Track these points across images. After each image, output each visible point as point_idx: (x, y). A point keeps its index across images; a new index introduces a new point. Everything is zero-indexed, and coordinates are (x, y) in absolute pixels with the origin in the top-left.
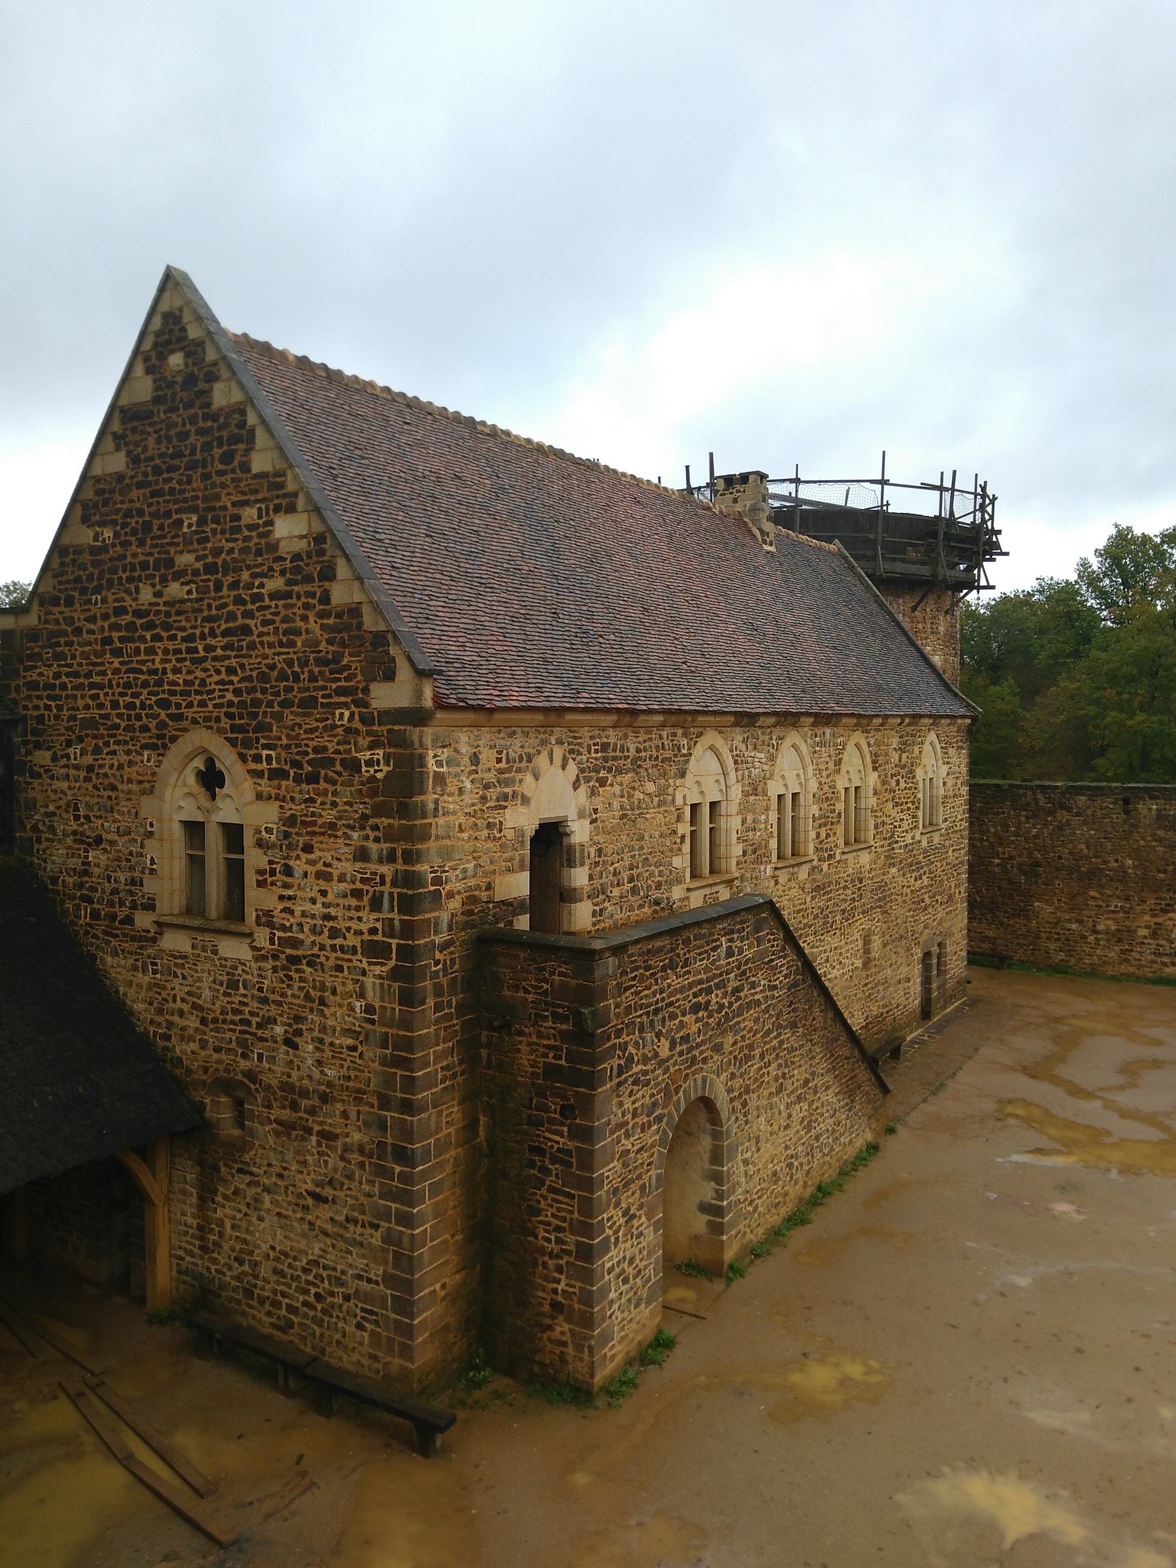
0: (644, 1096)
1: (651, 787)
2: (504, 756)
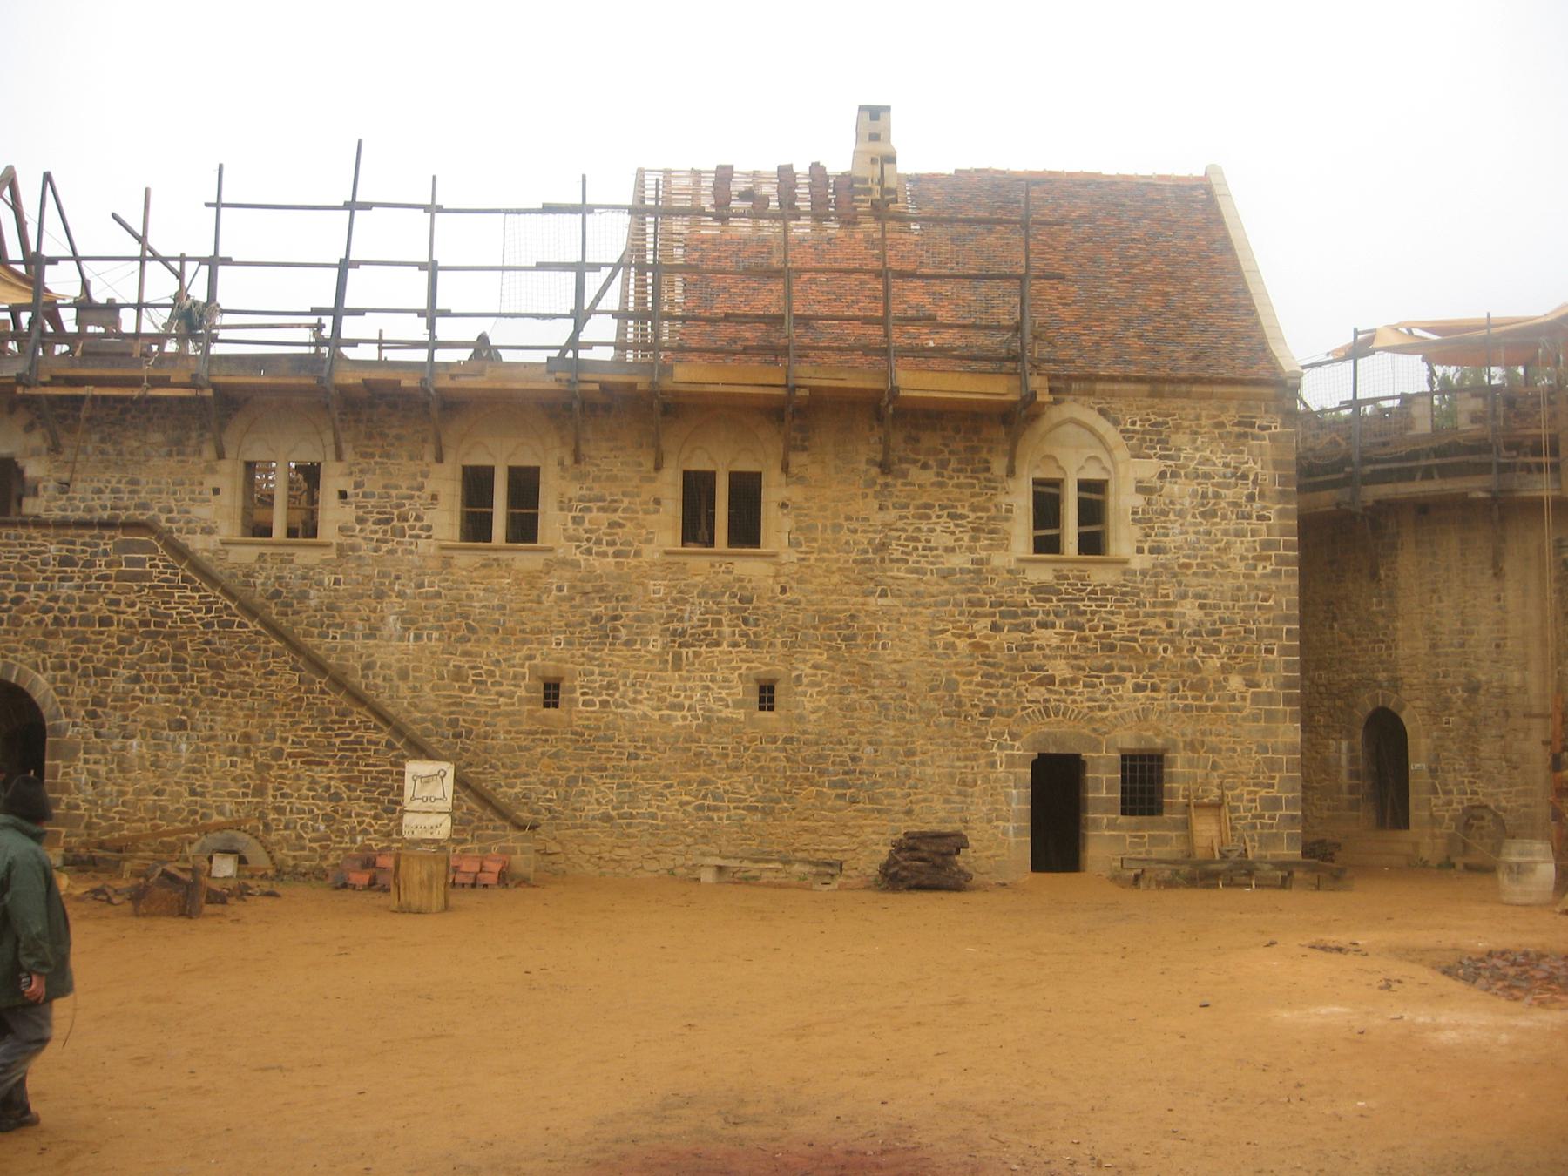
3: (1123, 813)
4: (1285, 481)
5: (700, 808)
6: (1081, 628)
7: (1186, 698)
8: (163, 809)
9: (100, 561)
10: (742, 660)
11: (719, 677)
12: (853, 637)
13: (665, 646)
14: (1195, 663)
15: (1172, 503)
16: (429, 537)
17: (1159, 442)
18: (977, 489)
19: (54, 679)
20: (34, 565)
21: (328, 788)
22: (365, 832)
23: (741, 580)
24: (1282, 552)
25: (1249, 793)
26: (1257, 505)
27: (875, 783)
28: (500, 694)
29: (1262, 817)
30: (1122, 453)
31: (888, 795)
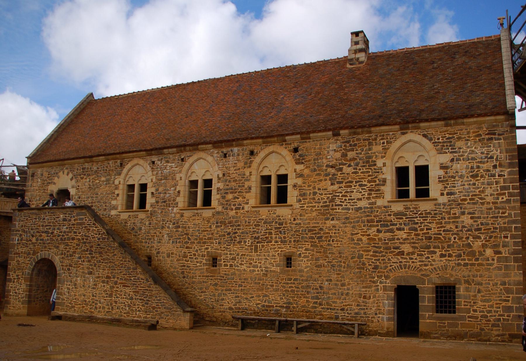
0: (25, 250)
1: (103, 179)
3: (437, 312)
4: (512, 158)
5: (263, 306)
6: (416, 230)
7: (464, 260)
8: (85, 301)
9: (73, 219)
10: (279, 248)
11: (271, 254)
12: (321, 237)
13: (252, 243)
14: (469, 244)
15: (457, 172)
16: (177, 207)
17: (450, 146)
18: (371, 174)
21: (129, 295)
22: (139, 311)
23: (280, 216)
24: (511, 191)
25: (497, 304)
26: (498, 169)
27: (329, 297)
28: (197, 262)
29: (504, 315)
30: (434, 152)
31: (334, 302)
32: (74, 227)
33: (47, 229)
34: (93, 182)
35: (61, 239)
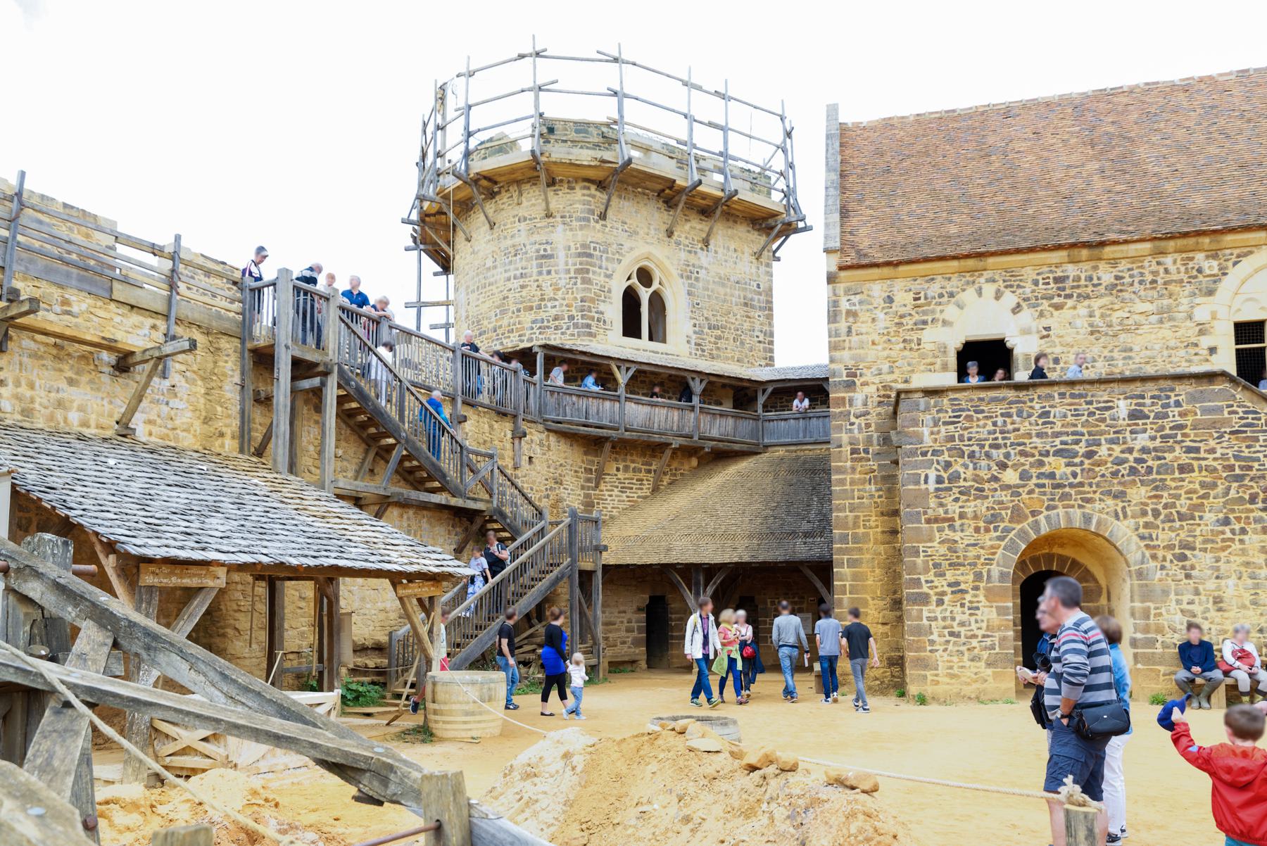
2: (922, 295)
19: (1138, 524)
20: (1103, 420)
32: (1184, 435)
33: (1062, 443)
34: (1102, 316)
35: (1133, 471)
